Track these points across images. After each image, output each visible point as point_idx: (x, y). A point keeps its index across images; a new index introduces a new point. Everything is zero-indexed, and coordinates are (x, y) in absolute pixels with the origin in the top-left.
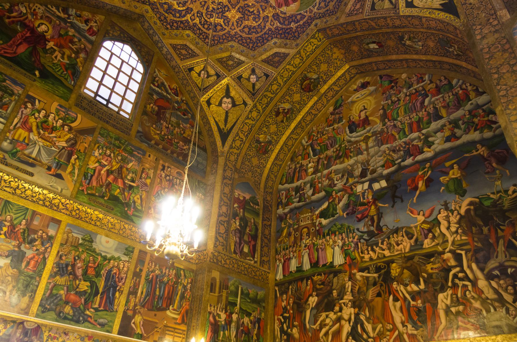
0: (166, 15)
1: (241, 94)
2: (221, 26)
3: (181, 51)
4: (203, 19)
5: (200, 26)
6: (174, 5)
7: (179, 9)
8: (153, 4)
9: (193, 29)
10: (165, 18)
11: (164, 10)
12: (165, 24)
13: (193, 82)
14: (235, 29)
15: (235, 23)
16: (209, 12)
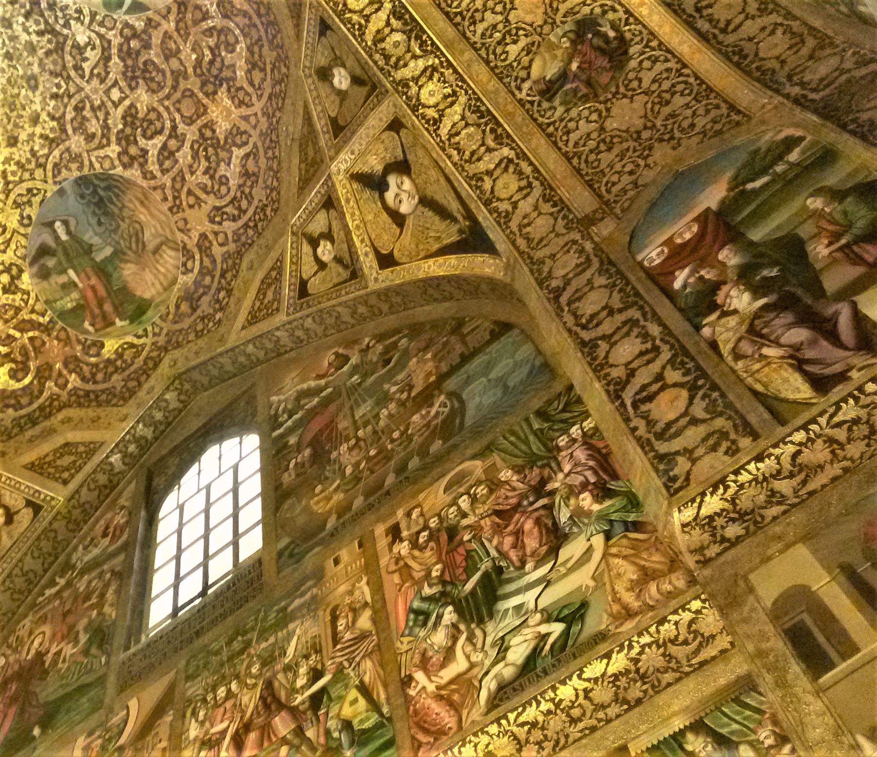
0: (199, 312)
1: (372, 132)
2: (247, 156)
3: (266, 301)
4: (227, 210)
5: (240, 223)
6: (185, 283)
7: (196, 271)
8: (169, 342)
9: (243, 245)
10: (202, 319)
11: (189, 316)
12: (211, 324)
13: (328, 295)
14: (256, 114)
15: (244, 111)
16: (213, 187)
